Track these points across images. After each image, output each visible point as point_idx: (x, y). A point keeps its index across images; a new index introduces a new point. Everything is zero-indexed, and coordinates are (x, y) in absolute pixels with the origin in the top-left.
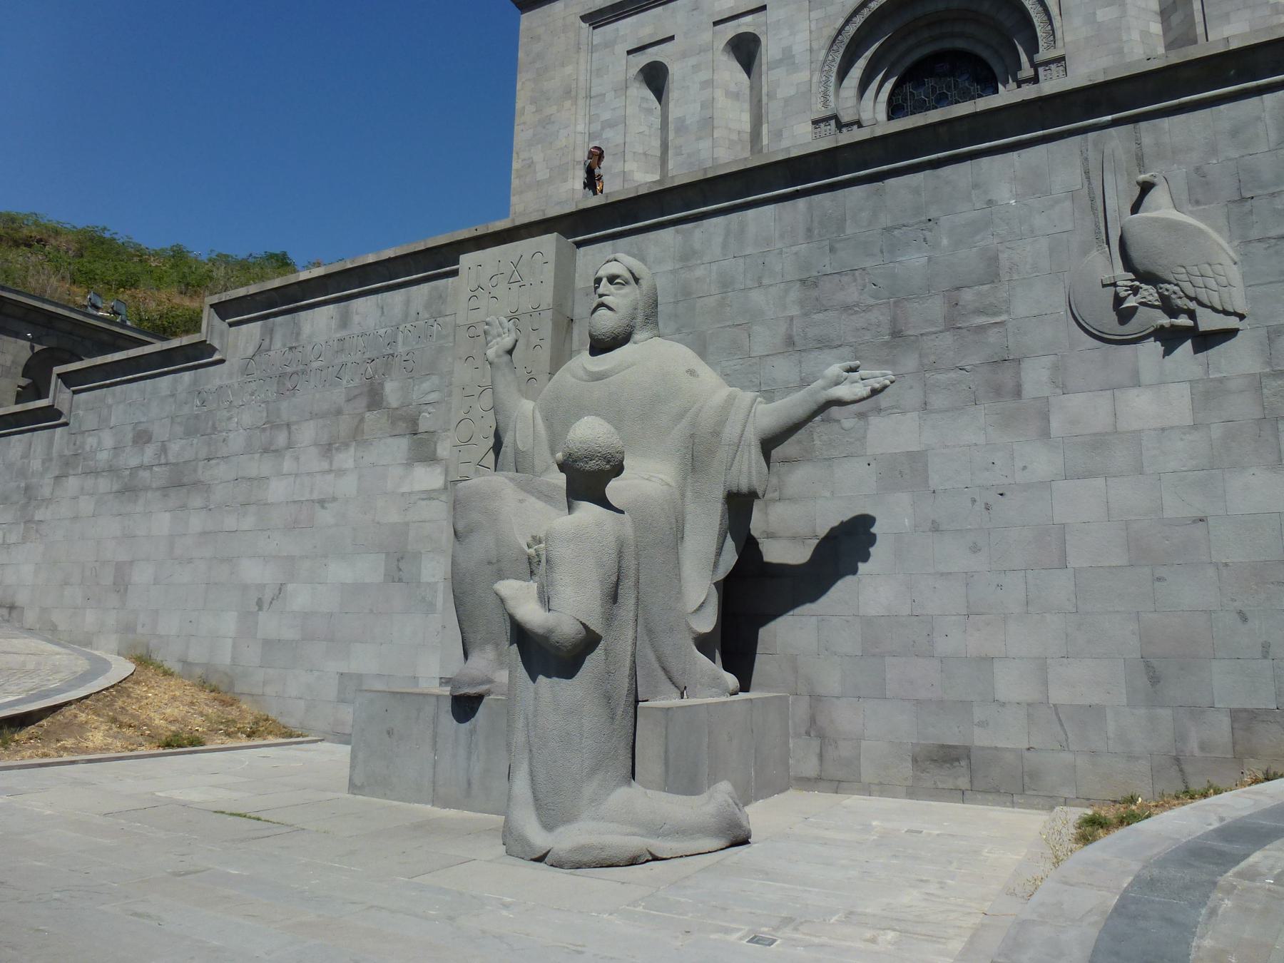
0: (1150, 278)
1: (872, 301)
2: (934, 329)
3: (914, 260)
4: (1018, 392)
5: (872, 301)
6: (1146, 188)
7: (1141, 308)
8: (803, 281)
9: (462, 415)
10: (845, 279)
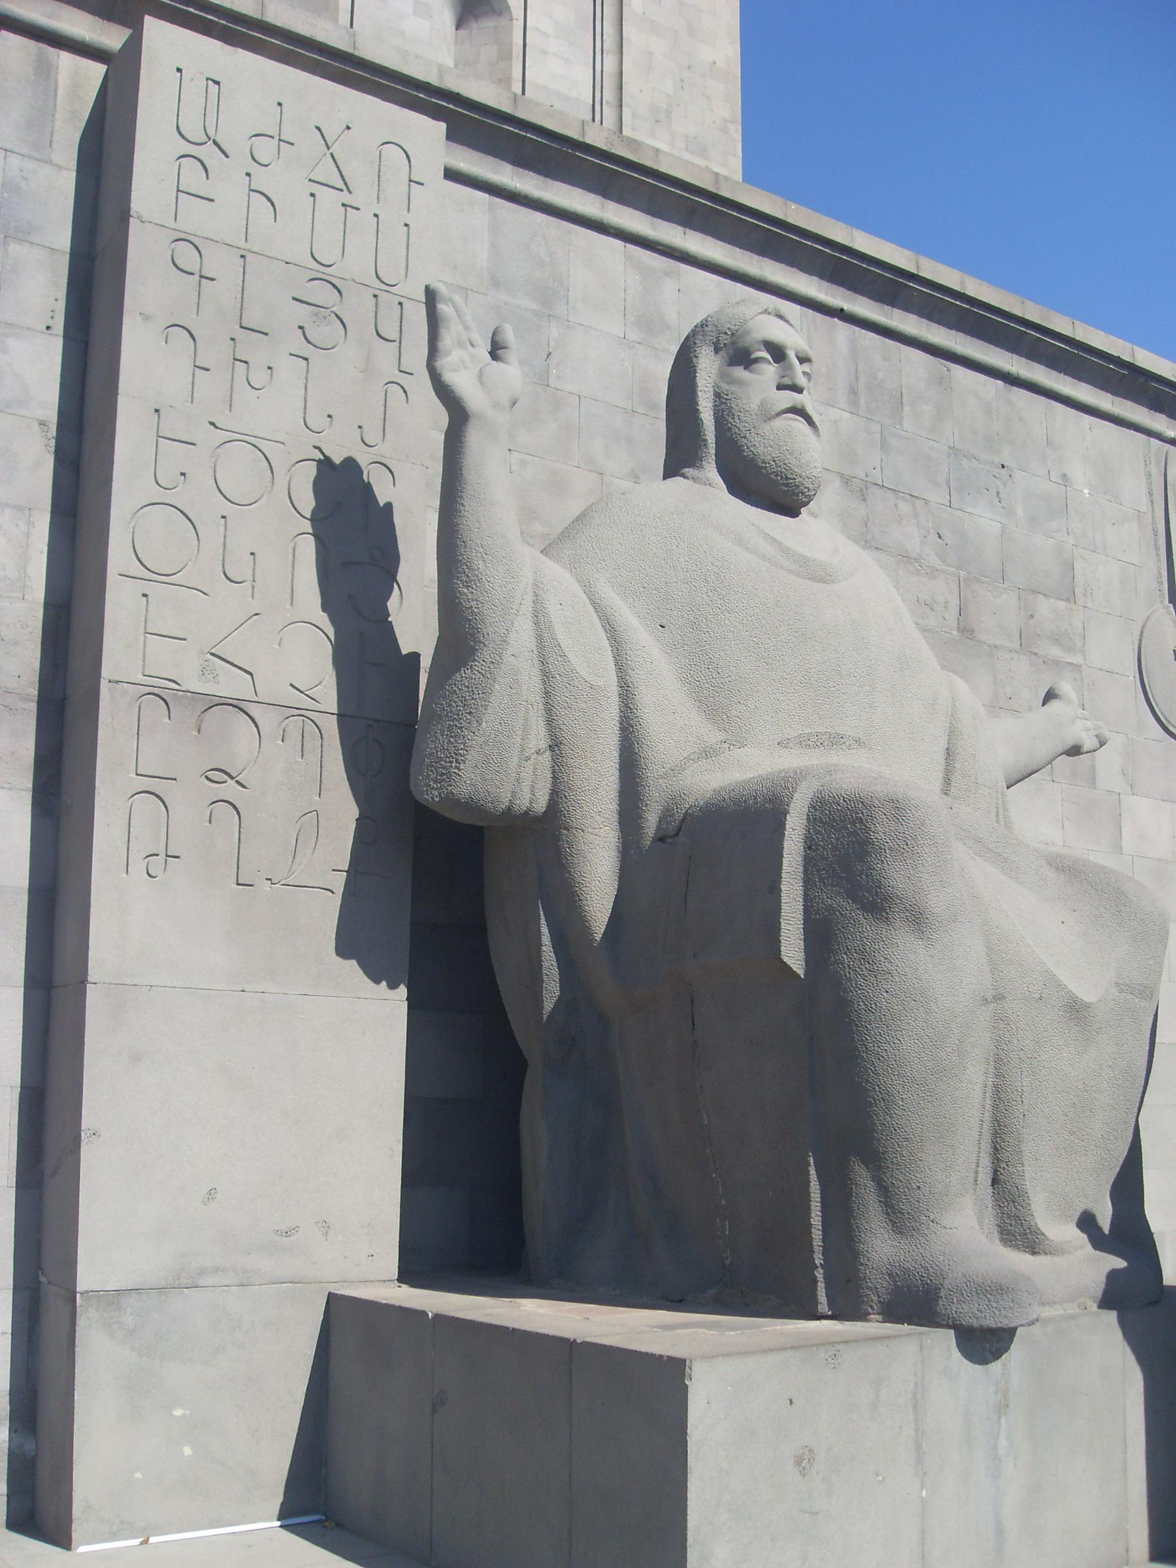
1: (936, 562)
2: (1009, 644)
3: (985, 521)
4: (1092, 781)
5: (936, 562)
8: (846, 480)
9: (157, 494)
10: (904, 507)
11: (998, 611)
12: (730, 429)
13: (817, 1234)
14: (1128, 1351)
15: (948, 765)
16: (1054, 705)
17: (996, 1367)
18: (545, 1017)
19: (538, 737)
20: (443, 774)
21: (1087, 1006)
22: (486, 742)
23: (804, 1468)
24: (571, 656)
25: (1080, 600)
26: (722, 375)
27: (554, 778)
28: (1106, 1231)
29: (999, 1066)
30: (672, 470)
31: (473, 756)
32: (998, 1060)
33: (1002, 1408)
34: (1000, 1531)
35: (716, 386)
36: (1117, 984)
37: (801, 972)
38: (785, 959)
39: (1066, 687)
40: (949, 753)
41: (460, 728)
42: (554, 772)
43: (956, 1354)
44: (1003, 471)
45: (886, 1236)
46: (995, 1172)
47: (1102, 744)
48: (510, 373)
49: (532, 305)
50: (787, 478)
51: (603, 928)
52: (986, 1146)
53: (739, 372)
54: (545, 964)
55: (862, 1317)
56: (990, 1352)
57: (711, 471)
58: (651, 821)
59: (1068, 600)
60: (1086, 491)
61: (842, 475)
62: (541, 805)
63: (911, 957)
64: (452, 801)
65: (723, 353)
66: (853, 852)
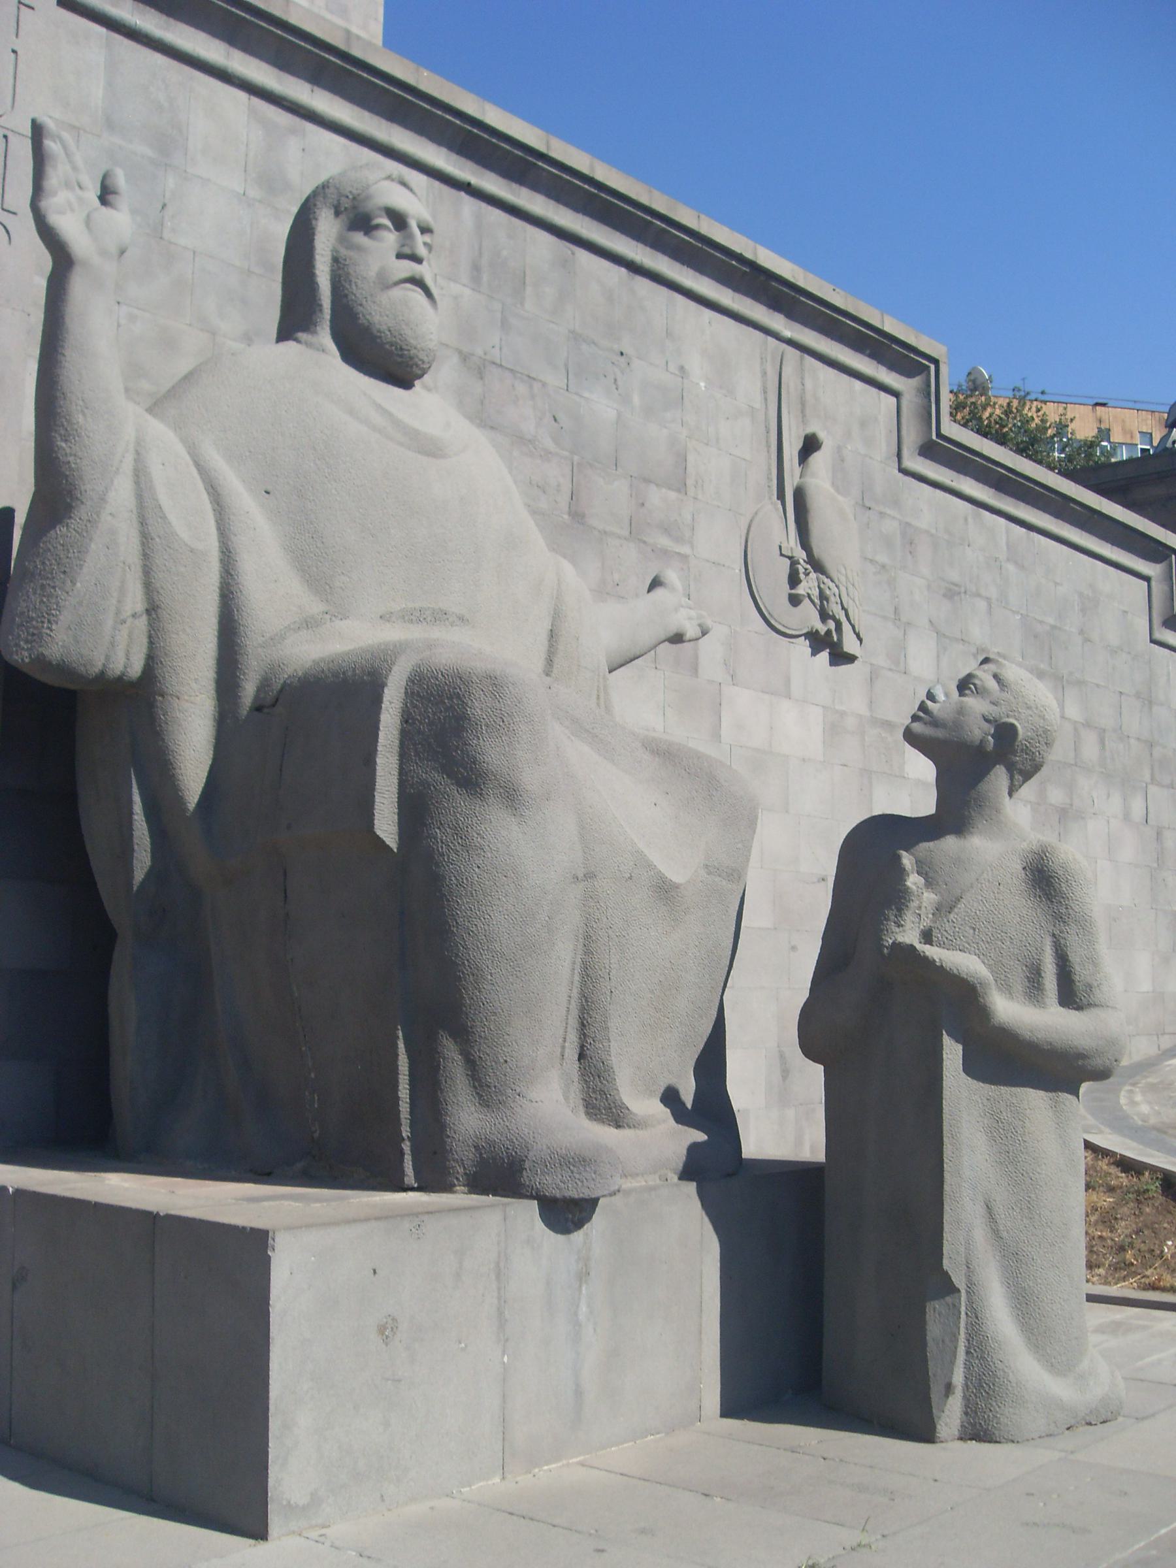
0: (818, 566)
3: (601, 406)
4: (695, 670)
6: (810, 445)
7: (807, 601)
8: (465, 358)
10: (522, 389)
11: (610, 496)
12: (346, 296)
13: (404, 1108)
14: (706, 1219)
15: (551, 646)
16: (659, 592)
17: (578, 1236)
18: (135, 888)
19: (135, 600)
20: (33, 634)
21: (677, 887)
22: (80, 603)
23: (387, 1337)
24: (172, 517)
25: (691, 491)
26: (342, 239)
27: (151, 642)
28: (689, 1106)
29: (588, 944)
30: (286, 333)
31: (65, 617)
32: (587, 937)
33: (583, 1276)
34: (579, 1393)
35: (334, 250)
36: (706, 866)
37: (393, 845)
38: (379, 833)
39: (672, 576)
40: (552, 635)
41: (54, 587)
42: (150, 637)
43: (539, 1224)
44: (622, 359)
45: (473, 1109)
46: (582, 1047)
47: (704, 633)
48: (120, 221)
49: (149, 152)
50: (401, 349)
51: (196, 801)
52: (573, 1022)
53: (359, 238)
54: (136, 834)
55: (448, 1188)
56: (573, 1222)
57: (325, 337)
58: (249, 690)
59: (679, 491)
60: (702, 384)
61: (460, 352)
62: (136, 669)
63: (504, 833)
64: (42, 662)
65: (343, 217)
66: (450, 728)
